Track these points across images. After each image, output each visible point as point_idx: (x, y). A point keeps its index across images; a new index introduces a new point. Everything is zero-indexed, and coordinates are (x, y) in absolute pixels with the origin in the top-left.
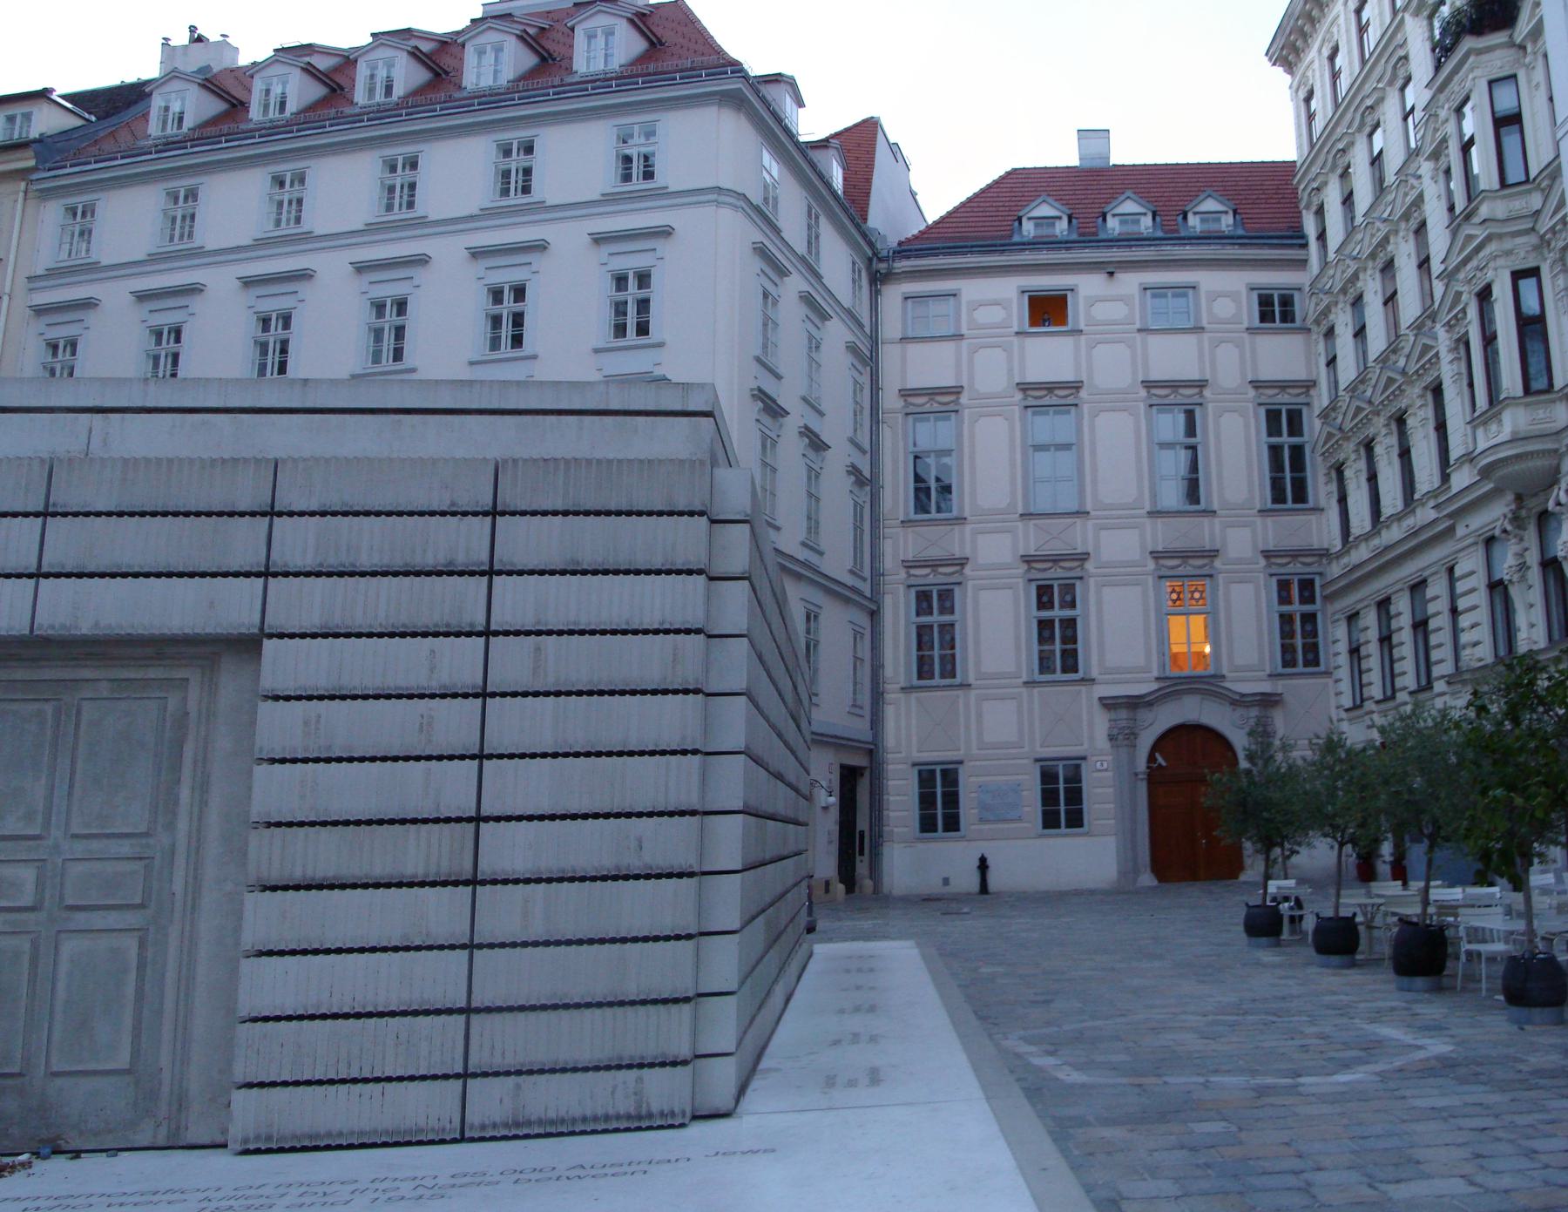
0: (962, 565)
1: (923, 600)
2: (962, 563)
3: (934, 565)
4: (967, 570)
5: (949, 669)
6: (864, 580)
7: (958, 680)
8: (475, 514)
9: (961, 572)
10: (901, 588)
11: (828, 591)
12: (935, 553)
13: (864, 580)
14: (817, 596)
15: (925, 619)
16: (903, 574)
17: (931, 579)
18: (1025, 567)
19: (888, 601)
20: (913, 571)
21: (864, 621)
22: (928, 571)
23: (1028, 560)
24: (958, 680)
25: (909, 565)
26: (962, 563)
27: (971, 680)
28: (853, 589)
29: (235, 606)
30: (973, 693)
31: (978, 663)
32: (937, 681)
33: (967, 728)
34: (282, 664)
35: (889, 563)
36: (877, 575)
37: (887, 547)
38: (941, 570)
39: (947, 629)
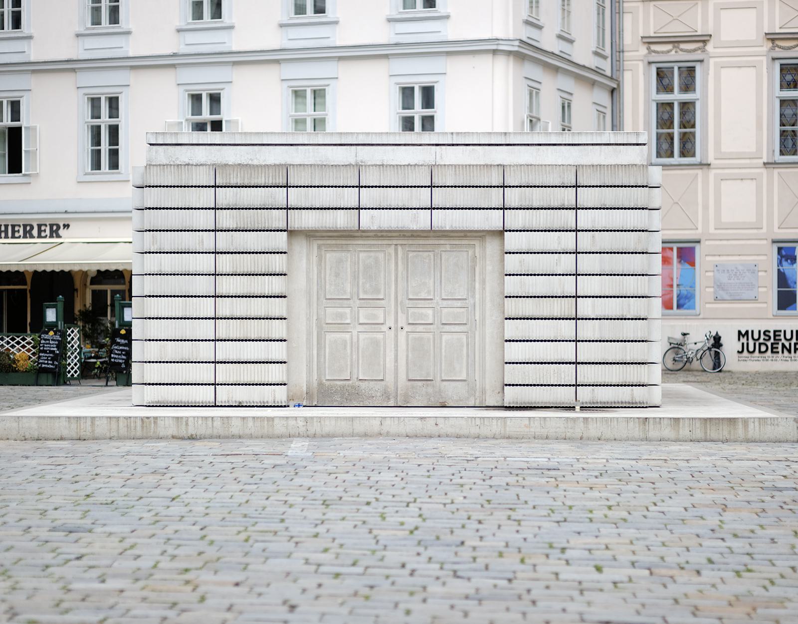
0: (704, 42)
1: (663, 78)
2: (704, 40)
3: (675, 42)
4: (710, 47)
5: (687, 149)
6: (605, 58)
7: (697, 159)
8: (570, 187)
9: (703, 50)
10: (641, 66)
11: (578, 78)
12: (676, 29)
13: (605, 58)
14: (568, 84)
15: (665, 97)
16: (643, 50)
17: (673, 56)
18: (770, 44)
19: (627, 79)
20: (653, 47)
21: (604, 98)
22: (670, 47)
23: (773, 38)
24: (697, 159)
25: (649, 41)
26: (704, 40)
27: (711, 159)
28: (597, 71)
29: (494, 220)
30: (712, 173)
31: (718, 143)
32: (677, 159)
33: (706, 207)
34: (512, 241)
35: (629, 39)
36: (618, 51)
37: (627, 20)
38: (682, 46)
39: (687, 107)
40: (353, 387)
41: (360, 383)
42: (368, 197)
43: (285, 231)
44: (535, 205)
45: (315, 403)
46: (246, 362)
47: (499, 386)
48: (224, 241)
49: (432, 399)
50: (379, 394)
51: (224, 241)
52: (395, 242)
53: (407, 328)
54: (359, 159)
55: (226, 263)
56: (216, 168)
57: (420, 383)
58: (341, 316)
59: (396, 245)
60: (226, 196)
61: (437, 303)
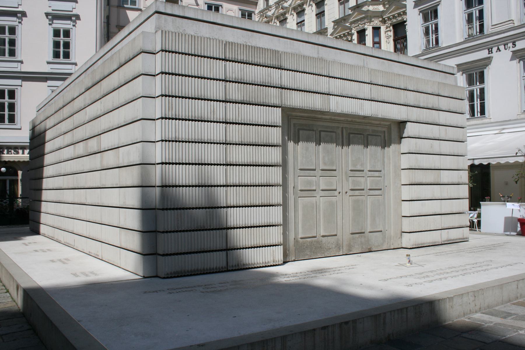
34: (410, 129)
40: (318, 242)
41: (323, 238)
42: (336, 86)
43: (279, 107)
44: (421, 105)
45: (293, 259)
46: (251, 227)
47: (399, 232)
48: (233, 112)
49: (364, 247)
50: (334, 246)
51: (233, 112)
52: (341, 125)
53: (350, 193)
54: (320, 56)
55: (235, 133)
56: (227, 44)
57: (357, 235)
58: (310, 183)
59: (342, 128)
60: (234, 70)
61: (366, 173)
